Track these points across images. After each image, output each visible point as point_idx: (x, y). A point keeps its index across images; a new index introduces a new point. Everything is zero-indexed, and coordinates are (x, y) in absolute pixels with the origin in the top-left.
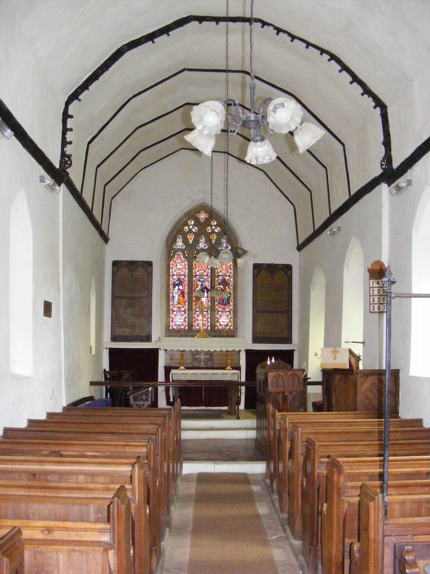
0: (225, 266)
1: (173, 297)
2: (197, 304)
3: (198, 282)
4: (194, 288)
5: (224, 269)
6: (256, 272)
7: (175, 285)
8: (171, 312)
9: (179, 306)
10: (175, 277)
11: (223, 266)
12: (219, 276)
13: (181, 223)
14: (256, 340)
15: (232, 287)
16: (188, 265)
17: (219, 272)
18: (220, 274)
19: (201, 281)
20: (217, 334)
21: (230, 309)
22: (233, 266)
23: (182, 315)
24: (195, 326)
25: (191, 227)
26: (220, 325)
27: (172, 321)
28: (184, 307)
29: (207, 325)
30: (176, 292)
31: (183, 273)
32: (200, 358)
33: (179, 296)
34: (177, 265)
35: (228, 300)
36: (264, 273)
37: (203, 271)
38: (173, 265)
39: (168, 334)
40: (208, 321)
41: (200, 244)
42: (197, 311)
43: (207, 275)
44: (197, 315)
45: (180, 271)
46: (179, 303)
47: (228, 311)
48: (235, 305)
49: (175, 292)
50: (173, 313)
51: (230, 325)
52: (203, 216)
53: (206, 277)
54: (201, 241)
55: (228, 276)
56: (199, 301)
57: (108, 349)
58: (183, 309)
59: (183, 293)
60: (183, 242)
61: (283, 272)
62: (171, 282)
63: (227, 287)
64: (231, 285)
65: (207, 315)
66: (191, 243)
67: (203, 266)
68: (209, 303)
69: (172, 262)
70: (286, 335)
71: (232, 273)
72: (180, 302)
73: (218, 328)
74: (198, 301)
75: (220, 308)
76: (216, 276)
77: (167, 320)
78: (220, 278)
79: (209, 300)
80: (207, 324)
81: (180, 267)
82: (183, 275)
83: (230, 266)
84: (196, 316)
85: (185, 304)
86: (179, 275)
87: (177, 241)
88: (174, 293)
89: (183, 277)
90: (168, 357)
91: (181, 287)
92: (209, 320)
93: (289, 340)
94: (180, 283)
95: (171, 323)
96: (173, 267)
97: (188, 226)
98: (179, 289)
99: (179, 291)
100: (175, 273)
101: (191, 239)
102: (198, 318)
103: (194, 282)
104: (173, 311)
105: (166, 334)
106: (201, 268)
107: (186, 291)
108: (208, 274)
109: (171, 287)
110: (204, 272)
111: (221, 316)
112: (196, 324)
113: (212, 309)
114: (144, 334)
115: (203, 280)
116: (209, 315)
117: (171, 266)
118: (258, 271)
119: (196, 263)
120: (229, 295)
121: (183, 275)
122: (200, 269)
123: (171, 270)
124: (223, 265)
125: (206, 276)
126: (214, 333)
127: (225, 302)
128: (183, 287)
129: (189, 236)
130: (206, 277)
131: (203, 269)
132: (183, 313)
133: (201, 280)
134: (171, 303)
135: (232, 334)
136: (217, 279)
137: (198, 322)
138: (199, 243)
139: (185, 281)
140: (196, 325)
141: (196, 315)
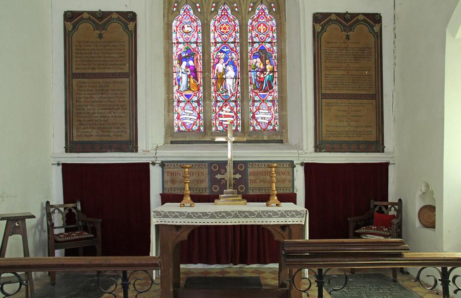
0: (264, 27)
1: (179, 80)
3: (219, 54)
4: (214, 63)
6: (318, 28)
7: (181, 60)
8: (175, 103)
9: (188, 93)
10: (181, 46)
12: (253, 43)
14: (318, 148)
15: (276, 61)
16: (203, 26)
20: (253, 139)
22: (276, 26)
23: (194, 109)
24: (216, 126)
26: (259, 123)
27: (178, 118)
28: (197, 94)
29: (235, 124)
30: (183, 71)
31: (193, 40)
32: (224, 179)
33: (189, 76)
34: (183, 27)
35: (269, 82)
36: (333, 28)
37: (227, 36)
38: (177, 27)
43: (234, 42)
45: (189, 36)
46: (189, 89)
47: (270, 101)
48: (282, 91)
49: (181, 72)
50: (178, 106)
53: (232, 45)
55: (269, 43)
56: (222, 85)
57: (61, 167)
58: (195, 99)
59: (194, 71)
61: (365, 28)
62: (174, 55)
63: (267, 61)
64: (273, 58)
65: (235, 108)
67: (227, 27)
68: (239, 88)
69: (175, 21)
70: (373, 138)
71: (276, 37)
72: (190, 87)
74: (219, 85)
75: (257, 95)
76: (250, 43)
77: (169, 115)
80: (235, 122)
81: (190, 29)
83: (272, 27)
84: (217, 110)
85: (199, 90)
86: (187, 43)
89: (194, 46)
90: (167, 178)
91: (191, 63)
92: (239, 115)
93: (377, 145)
94: (190, 55)
95: (176, 121)
98: (188, 66)
99: (188, 70)
100: (181, 40)
102: (221, 112)
103: (212, 54)
104: (179, 102)
105: (166, 137)
106: (225, 31)
107: (200, 68)
108: (235, 39)
109: (175, 62)
110: (230, 36)
111: (258, 109)
112: (218, 122)
113: (243, 98)
114: (126, 137)
115: (227, 50)
116: (238, 108)
117: (174, 28)
118: (322, 26)
119: (215, 23)
122: (223, 32)
123: (174, 35)
124: (259, 25)
125: (232, 43)
126: (249, 136)
127: (264, 86)
128: (195, 61)
130: (233, 45)
132: (195, 104)
133: (223, 50)
134: (176, 88)
135: (279, 138)
136: (250, 48)
137: (220, 119)
139: (198, 52)
140: (217, 125)
141: (217, 108)
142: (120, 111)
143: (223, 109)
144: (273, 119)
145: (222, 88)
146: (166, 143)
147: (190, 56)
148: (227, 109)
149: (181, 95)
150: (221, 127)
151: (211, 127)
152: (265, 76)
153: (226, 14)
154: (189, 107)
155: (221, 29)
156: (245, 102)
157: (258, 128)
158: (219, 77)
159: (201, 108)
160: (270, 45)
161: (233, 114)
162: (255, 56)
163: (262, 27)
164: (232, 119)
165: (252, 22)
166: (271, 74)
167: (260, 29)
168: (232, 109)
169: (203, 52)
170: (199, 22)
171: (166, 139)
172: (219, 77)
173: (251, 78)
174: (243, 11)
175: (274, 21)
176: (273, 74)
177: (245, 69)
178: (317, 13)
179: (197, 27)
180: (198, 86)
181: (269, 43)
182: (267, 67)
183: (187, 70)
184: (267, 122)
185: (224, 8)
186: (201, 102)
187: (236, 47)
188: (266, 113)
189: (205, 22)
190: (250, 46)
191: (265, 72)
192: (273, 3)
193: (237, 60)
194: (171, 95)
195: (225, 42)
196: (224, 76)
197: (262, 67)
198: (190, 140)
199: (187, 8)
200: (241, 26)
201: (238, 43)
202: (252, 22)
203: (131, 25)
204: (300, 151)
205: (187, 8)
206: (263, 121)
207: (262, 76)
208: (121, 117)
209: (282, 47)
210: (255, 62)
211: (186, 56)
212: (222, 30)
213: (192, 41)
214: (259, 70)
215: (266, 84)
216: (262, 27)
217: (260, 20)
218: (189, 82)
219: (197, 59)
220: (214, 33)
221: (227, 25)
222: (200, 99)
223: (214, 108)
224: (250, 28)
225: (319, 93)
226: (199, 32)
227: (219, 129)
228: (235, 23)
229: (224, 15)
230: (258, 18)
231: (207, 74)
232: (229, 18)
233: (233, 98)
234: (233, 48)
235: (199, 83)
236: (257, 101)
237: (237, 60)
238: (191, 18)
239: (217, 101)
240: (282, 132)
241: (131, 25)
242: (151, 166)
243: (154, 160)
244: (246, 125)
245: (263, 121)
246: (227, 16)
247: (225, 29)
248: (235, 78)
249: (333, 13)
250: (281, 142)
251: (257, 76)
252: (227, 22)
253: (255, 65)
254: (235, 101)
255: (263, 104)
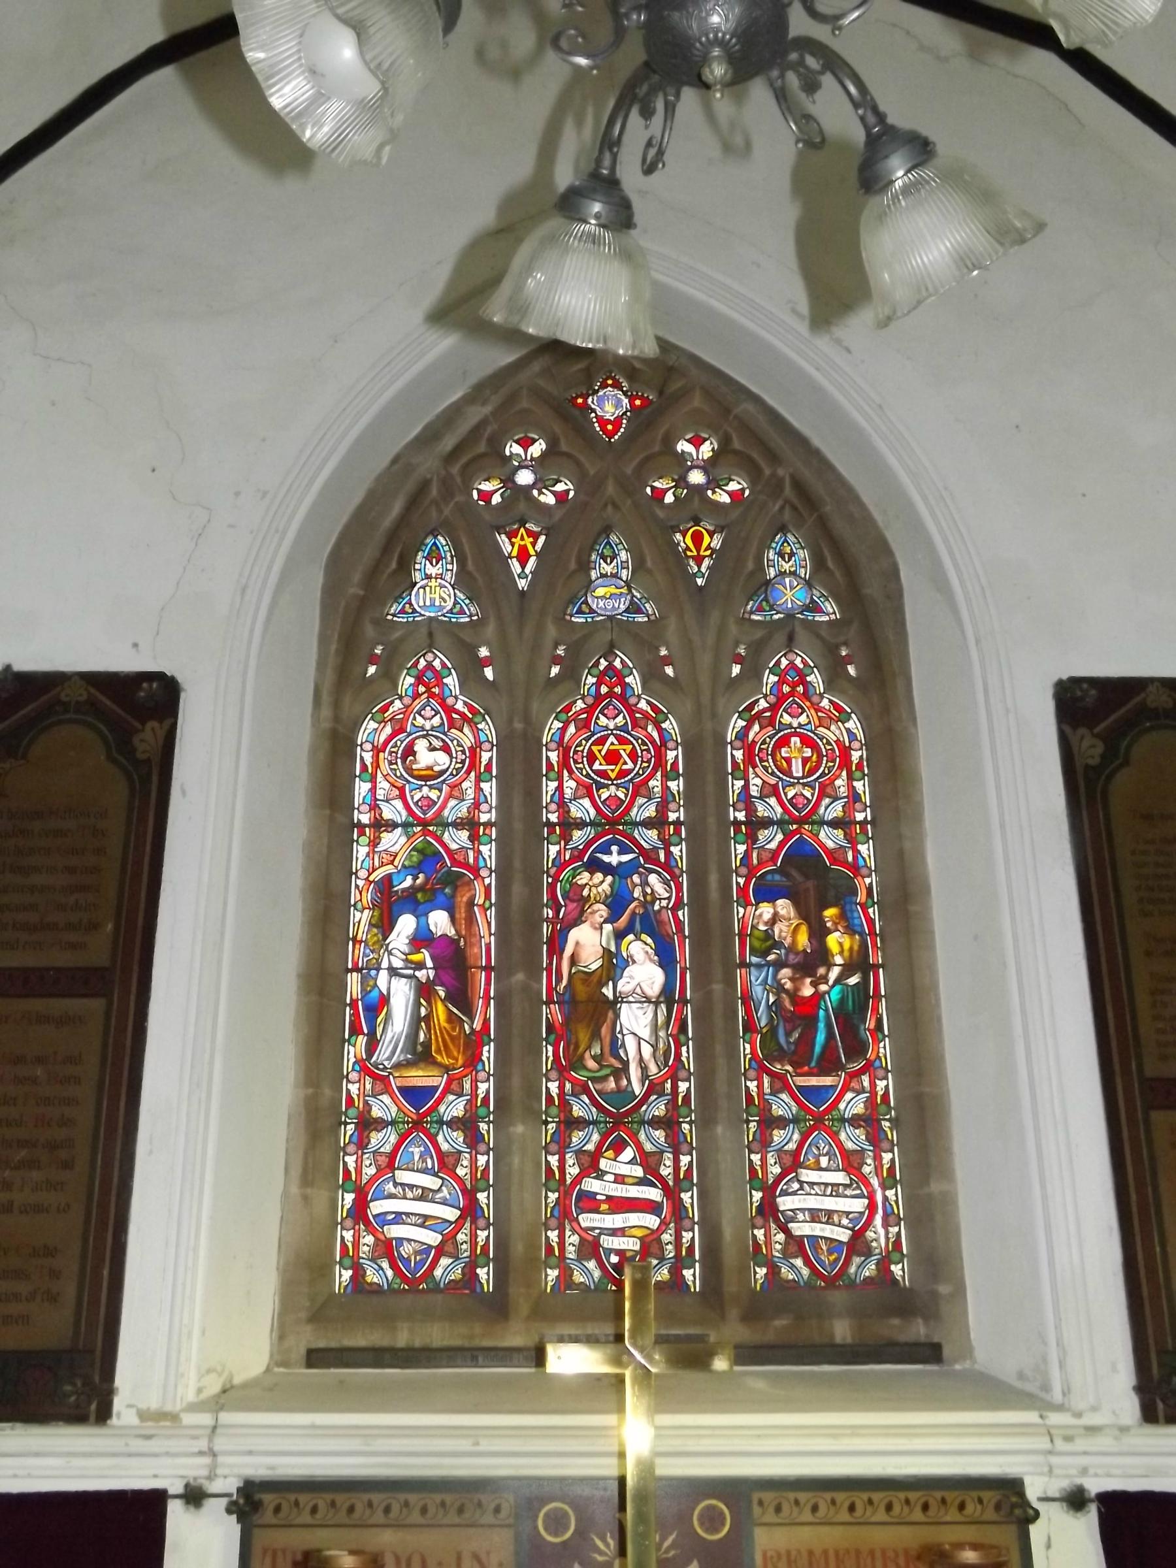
0: (808, 752)
2: (577, 1063)
3: (583, 878)
4: (553, 922)
5: (797, 770)
6: (1091, 749)
9: (420, 1077)
10: (393, 840)
11: (784, 752)
12: (755, 824)
13: (449, 443)
17: (754, 791)
18: (761, 810)
19: (607, 869)
20: (770, 1337)
21: (871, 1103)
22: (868, 745)
25: (525, 477)
26: (796, 1246)
27: (359, 1212)
28: (467, 1086)
30: (397, 963)
31: (455, 810)
33: (424, 991)
34: (410, 751)
38: (377, 750)
39: (307, 1338)
40: (678, 1211)
41: (600, 592)
42: (581, 1123)
44: (579, 1153)
45: (434, 795)
51: (878, 1235)
52: (618, 404)
54: (608, 569)
55: (835, 824)
56: (596, 1035)
58: (454, 1107)
60: (463, 581)
63: (830, 913)
64: (861, 897)
66: (522, 584)
68: (687, 1053)
72: (427, 1045)
73: (773, 1270)
74: (583, 1036)
75: (787, 1087)
76: (737, 823)
77: (305, 1198)
78: (771, 839)
79: (683, 1028)
82: (458, 825)
83: (845, 752)
84: (573, 1171)
85: (474, 1060)
86: (424, 823)
87: (417, 576)
88: (385, 964)
89: (457, 839)
91: (439, 922)
96: (377, 765)
97: (506, 470)
98: (420, 940)
99: (425, 956)
100: (393, 811)
101: (523, 557)
102: (591, 1185)
103: (546, 880)
104: (367, 1124)
105: (282, 1332)
106: (612, 770)
108: (663, 808)
109: (361, 920)
111: (793, 1163)
116: (685, 1160)
118: (1105, 737)
120: (853, 980)
121: (458, 825)
122: (603, 774)
123: (362, 788)
124: (784, 742)
125: (648, 824)
127: (821, 1038)
128: (461, 914)
129: (511, 535)
130: (653, 834)
131: (623, 774)
132: (451, 1140)
133: (606, 858)
136: (741, 848)
138: (589, 586)
139: (475, 870)
141: (570, 1159)
142: (36, 1175)
143: (603, 1164)
144: (878, 1220)
145: (596, 1050)
146: (280, 1359)
147: (434, 891)
148: (624, 1163)
149: (379, 1086)
150: (592, 1265)
151: (534, 1266)
152: (823, 988)
153: (618, 690)
154: (417, 1151)
155: (592, 758)
156: (719, 1130)
157: (796, 1270)
158: (581, 991)
159: (482, 1160)
160: (840, 833)
161: (654, 1194)
162: (767, 894)
163: (795, 751)
164: (652, 1221)
165: (747, 728)
166: (853, 980)
167: (788, 760)
168: (649, 1162)
169: (503, 871)
170: (488, 729)
171: (282, 1338)
172: (581, 991)
173: (747, 998)
174: (704, 678)
175: (853, 724)
176: (865, 980)
177: (716, 956)
178: (1076, 681)
179: (474, 752)
180: (474, 1044)
181: (835, 824)
182: (833, 940)
183: (416, 957)
184: (844, 1235)
185: (610, 667)
186: (483, 1127)
187: (667, 845)
188: (835, 1190)
189: (518, 725)
190: (741, 837)
191: (821, 971)
192: (846, 644)
193: (675, 909)
194: (328, 1092)
195: (613, 822)
196: (608, 992)
197: (803, 940)
198: (417, 1343)
199: (429, 666)
200: (691, 748)
201: (677, 823)
202: (747, 728)
203: (147, 734)
204: (1055, 1418)
205: (429, 666)
206: (818, 1229)
207: (807, 991)
208: (39, 1209)
209: (907, 845)
210: (767, 916)
211: (413, 890)
212: (596, 766)
213: (449, 814)
214: (792, 959)
215: (829, 1026)
216: (795, 751)
217: (787, 719)
218: (428, 1018)
219: (471, 904)
220: (560, 779)
221: (622, 741)
222: (482, 1111)
223: (554, 1160)
224: (739, 755)
225: (1126, 1071)
226: (486, 776)
227: (578, 1278)
228: (660, 730)
229: (610, 694)
230: (774, 708)
231: (520, 977)
232: (631, 710)
233: (658, 1108)
234: (655, 849)
235: (477, 1025)
236: (782, 1122)
237: (675, 909)
238: (449, 710)
239: (571, 1123)
240: (934, 1295)
241: (147, 738)
242: (175, 1511)
243: (193, 1469)
244: (730, 1256)
245: (818, 1229)
246: (623, 698)
247: (612, 757)
248: (667, 994)
249: (1152, 680)
250: (931, 1353)
251: (779, 988)
252: (623, 728)
253: (768, 935)
254: (669, 1123)
255: (821, 1140)
